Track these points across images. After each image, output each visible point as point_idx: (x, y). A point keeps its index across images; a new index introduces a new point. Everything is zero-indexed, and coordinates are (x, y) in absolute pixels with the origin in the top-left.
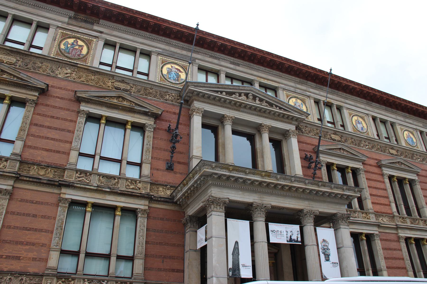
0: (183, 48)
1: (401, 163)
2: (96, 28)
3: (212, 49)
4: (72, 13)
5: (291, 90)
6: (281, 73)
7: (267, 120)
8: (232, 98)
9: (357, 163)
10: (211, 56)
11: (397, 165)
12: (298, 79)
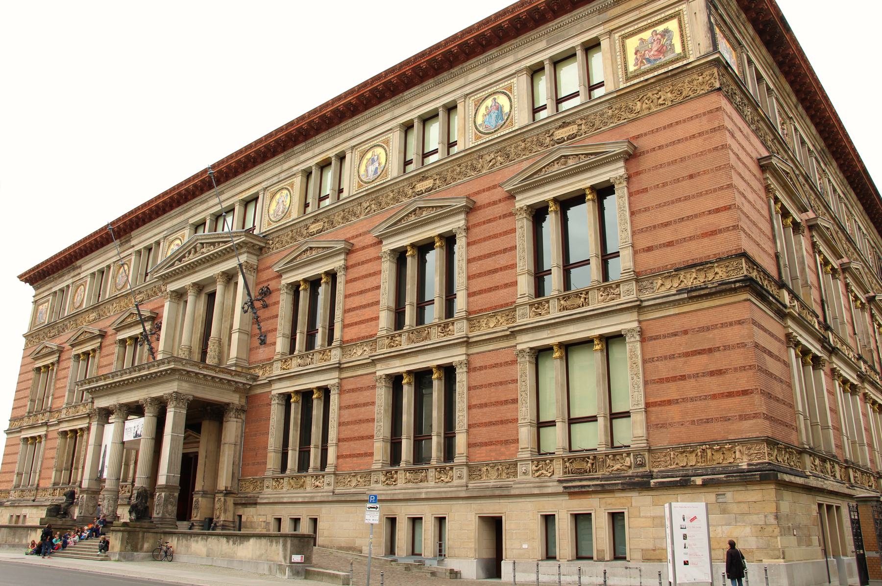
0: (181, 214)
1: (420, 208)
2: (133, 243)
3: (194, 196)
4: (117, 242)
6: (262, 165)
7: (220, 265)
8: (187, 261)
9: (335, 259)
10: (202, 203)
12: (281, 156)
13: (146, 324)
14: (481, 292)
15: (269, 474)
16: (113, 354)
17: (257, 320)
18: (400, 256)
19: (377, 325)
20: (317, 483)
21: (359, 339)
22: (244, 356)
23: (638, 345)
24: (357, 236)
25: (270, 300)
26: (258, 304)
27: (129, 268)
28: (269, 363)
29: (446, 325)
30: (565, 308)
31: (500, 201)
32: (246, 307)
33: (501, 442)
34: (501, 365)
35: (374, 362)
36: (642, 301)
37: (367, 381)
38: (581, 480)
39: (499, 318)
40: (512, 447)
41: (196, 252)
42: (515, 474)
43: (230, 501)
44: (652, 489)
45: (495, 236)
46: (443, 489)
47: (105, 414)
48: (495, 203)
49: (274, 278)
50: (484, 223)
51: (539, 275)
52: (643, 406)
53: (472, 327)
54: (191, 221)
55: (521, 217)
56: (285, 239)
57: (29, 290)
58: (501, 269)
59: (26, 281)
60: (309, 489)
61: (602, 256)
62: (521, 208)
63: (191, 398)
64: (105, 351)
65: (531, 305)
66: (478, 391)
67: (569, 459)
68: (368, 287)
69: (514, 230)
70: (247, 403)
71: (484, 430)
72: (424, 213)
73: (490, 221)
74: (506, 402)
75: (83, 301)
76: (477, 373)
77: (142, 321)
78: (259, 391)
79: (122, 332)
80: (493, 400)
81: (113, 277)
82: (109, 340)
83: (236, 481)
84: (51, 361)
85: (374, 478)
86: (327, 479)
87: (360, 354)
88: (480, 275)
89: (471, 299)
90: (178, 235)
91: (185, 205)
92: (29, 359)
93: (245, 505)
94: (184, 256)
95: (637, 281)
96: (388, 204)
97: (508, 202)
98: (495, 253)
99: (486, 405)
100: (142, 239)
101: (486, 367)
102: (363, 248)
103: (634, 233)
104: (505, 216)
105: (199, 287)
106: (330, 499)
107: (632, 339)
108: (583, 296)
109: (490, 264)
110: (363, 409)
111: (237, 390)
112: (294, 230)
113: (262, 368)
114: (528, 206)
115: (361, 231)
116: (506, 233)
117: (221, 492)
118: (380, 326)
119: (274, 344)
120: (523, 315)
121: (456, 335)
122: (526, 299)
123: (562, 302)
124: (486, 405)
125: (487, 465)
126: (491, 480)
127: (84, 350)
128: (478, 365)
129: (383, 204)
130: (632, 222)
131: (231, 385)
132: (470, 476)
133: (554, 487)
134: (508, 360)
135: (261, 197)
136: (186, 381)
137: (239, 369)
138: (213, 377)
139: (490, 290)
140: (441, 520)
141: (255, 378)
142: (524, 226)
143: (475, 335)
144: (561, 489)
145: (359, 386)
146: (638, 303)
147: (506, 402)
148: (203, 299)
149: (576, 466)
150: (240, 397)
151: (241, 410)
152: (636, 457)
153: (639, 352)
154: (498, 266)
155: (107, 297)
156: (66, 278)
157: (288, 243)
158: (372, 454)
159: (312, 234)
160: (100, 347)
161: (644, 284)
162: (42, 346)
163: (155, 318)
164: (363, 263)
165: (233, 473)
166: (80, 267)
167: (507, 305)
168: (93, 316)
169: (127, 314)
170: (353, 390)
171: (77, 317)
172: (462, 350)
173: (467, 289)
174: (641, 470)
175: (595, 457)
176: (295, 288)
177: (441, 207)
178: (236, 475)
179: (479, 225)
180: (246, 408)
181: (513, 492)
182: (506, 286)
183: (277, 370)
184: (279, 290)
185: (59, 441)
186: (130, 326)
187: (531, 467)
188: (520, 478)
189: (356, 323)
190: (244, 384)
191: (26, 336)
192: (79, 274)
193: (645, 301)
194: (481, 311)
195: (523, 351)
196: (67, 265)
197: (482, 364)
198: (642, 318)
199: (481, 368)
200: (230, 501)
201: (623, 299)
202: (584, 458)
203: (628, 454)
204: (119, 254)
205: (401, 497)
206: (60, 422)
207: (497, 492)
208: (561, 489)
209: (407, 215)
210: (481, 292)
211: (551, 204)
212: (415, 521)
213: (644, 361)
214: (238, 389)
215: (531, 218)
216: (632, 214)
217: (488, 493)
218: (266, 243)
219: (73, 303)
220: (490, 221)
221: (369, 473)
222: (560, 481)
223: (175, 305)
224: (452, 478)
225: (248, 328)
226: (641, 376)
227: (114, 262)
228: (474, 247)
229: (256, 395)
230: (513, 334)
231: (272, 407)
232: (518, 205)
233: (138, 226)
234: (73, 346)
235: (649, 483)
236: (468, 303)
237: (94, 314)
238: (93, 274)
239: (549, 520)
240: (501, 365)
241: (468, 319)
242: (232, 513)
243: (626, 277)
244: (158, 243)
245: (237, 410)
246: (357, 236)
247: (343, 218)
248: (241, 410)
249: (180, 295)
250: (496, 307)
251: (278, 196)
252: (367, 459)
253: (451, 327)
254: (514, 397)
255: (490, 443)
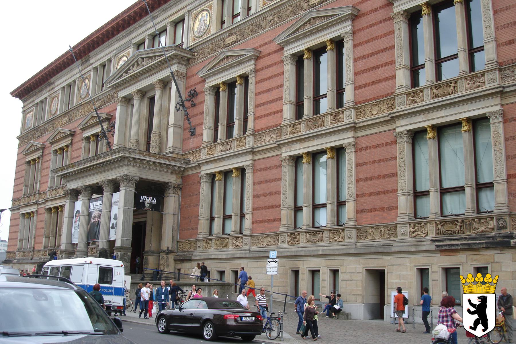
1: (314, 18)
2: (91, 61)
3: (135, 21)
4: (80, 61)
5: (196, 5)
7: (157, 74)
8: (131, 73)
9: (247, 65)
11: (308, 27)
13: (103, 124)
14: (366, 85)
15: (200, 236)
16: (81, 148)
17: (187, 117)
18: (298, 60)
19: (282, 116)
20: (237, 243)
21: (267, 128)
22: (179, 145)
23: (501, 126)
24: (264, 45)
25: (197, 100)
26: (187, 104)
27: (89, 81)
28: (198, 150)
29: (337, 114)
30: (437, 96)
31: (380, 8)
32: (178, 106)
33: (382, 209)
34: (383, 145)
35: (279, 146)
36: (504, 88)
37: (274, 162)
38: (451, 240)
39: (380, 106)
40: (393, 212)
41: (138, 65)
42: (395, 235)
43: (171, 258)
44: (512, 248)
45: (377, 38)
46: (337, 248)
47: (75, 194)
48: (376, 10)
49: (199, 83)
50: (367, 27)
51: (415, 69)
52: (505, 177)
53: (358, 115)
54: (134, 41)
55: (398, 20)
56: (206, 50)
57: (18, 103)
58: (382, 66)
59: (16, 96)
60: (230, 247)
61: (469, 51)
62: (399, 13)
63: (138, 179)
64: (75, 146)
65: (408, 94)
66: (364, 168)
67: (441, 223)
68: (273, 86)
69: (393, 32)
70: (182, 181)
71: (369, 199)
72: (317, 22)
73: (372, 25)
74: (388, 176)
75: (57, 109)
76: (364, 152)
77: (100, 122)
78: (190, 172)
79: (87, 131)
80: (377, 174)
81: (78, 89)
82: (77, 139)
83: (176, 243)
84: (37, 156)
85: (281, 239)
86: (245, 240)
87: (269, 140)
88: (365, 71)
89: (358, 91)
90: (125, 53)
91: (129, 29)
92: (22, 155)
93: (183, 261)
94: (129, 69)
95: (500, 70)
96: (287, 17)
97: (387, 8)
98: (377, 53)
99: (371, 178)
100: (98, 58)
101: (370, 148)
102: (269, 54)
103: (497, 29)
104: (385, 20)
105: (142, 93)
106: (247, 255)
107: (496, 121)
108: (452, 85)
109: (372, 61)
110: (272, 184)
111: (173, 172)
112: (214, 43)
113: (192, 154)
114: (405, 11)
115: (267, 40)
116: (385, 35)
117: (164, 252)
118: (284, 117)
119: (202, 135)
120: (401, 103)
121: (346, 122)
122: (403, 90)
123: (435, 91)
124: (371, 178)
125: (372, 227)
126: (375, 240)
127: (60, 146)
128: (364, 146)
129: (284, 17)
130: (495, 19)
131: (169, 168)
132: (358, 237)
133: (428, 246)
134: (389, 141)
135: (186, 18)
136: (134, 166)
137: (175, 156)
138: (154, 163)
139: (373, 83)
140: (335, 272)
141: (188, 162)
142: (401, 28)
143: (362, 121)
144: (433, 247)
145: (268, 165)
146: (501, 89)
147: (388, 176)
148: (146, 104)
149: (446, 228)
150: (176, 178)
151: (178, 188)
152: (498, 220)
153: (501, 131)
154: (379, 63)
155: (74, 105)
156: (44, 92)
157: (209, 53)
158: (279, 220)
159: (227, 46)
160: (71, 144)
161: (506, 72)
162: (30, 145)
163: (110, 119)
164: (269, 66)
165: (173, 237)
166: (54, 83)
167: (387, 95)
168: (65, 120)
169: (89, 117)
170: (264, 169)
171: (54, 122)
172: (351, 134)
173: (354, 83)
174: (503, 231)
175: (463, 221)
176: (216, 89)
177: (331, 16)
178: (175, 238)
179: (363, 29)
180: (181, 186)
181: (393, 249)
182: (387, 79)
183: (204, 156)
184: (204, 92)
185: (46, 216)
186: (92, 126)
187: (409, 229)
188: (399, 237)
189: (265, 116)
190: (179, 167)
191: (18, 138)
192: (53, 88)
193: (507, 87)
194: (366, 101)
195: (401, 133)
196: (44, 82)
197: (367, 145)
198: (505, 102)
199: (366, 148)
200: (171, 258)
201: (488, 86)
202: (454, 221)
203: (492, 219)
204: (81, 71)
205: (302, 253)
206: (46, 201)
207: (381, 250)
208: (433, 247)
209: (303, 25)
210: (366, 85)
211: (424, 8)
212: (314, 273)
213: (506, 139)
214: (174, 171)
215: (407, 21)
216: (495, 12)
217: (373, 250)
218: (192, 55)
219: (51, 111)
220: (372, 25)
221: (277, 235)
222: (433, 241)
223: (125, 108)
224: (343, 238)
225: (181, 123)
226: (503, 152)
227: (78, 78)
228: (359, 48)
229: (188, 175)
230: (393, 119)
231: (201, 184)
232: (395, 10)
233: (94, 48)
234: (52, 143)
235: (510, 242)
236: (355, 95)
237: (66, 119)
238: (64, 88)
239: (423, 272)
240: (383, 145)
241: (355, 108)
242: (173, 267)
243: (490, 67)
244: (110, 60)
245: (174, 187)
246: (264, 45)
247: (252, 31)
248: (178, 188)
249: (128, 100)
250: (378, 98)
251: (200, 17)
252: (275, 224)
253: (341, 116)
254: (393, 171)
255: (375, 210)
